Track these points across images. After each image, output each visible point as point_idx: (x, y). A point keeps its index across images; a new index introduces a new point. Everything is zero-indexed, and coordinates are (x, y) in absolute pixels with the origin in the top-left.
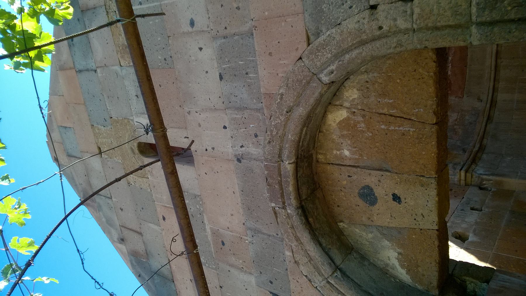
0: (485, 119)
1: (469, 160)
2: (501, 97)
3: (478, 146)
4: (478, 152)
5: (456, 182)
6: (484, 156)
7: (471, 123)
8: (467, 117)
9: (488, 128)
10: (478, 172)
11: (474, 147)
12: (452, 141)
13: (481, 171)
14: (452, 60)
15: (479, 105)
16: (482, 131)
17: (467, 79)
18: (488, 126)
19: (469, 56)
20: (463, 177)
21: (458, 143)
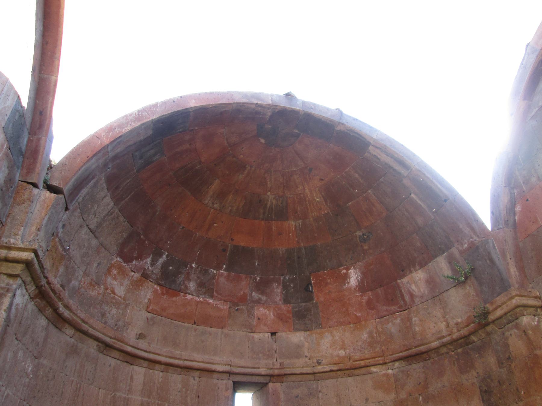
0: (108, 340)
1: (46, 285)
2: (139, 372)
3: (67, 314)
4: (55, 310)
5: (5, 240)
6: (43, 322)
7: (103, 315)
8: (114, 311)
9: (91, 341)
10: (18, 292)
11: (66, 307)
12: (81, 273)
13: (18, 300)
14: (209, 304)
15: (131, 335)
16: (90, 329)
17: (174, 322)
18: (96, 343)
19: (209, 329)
20: (14, 254)
21: (75, 283)
